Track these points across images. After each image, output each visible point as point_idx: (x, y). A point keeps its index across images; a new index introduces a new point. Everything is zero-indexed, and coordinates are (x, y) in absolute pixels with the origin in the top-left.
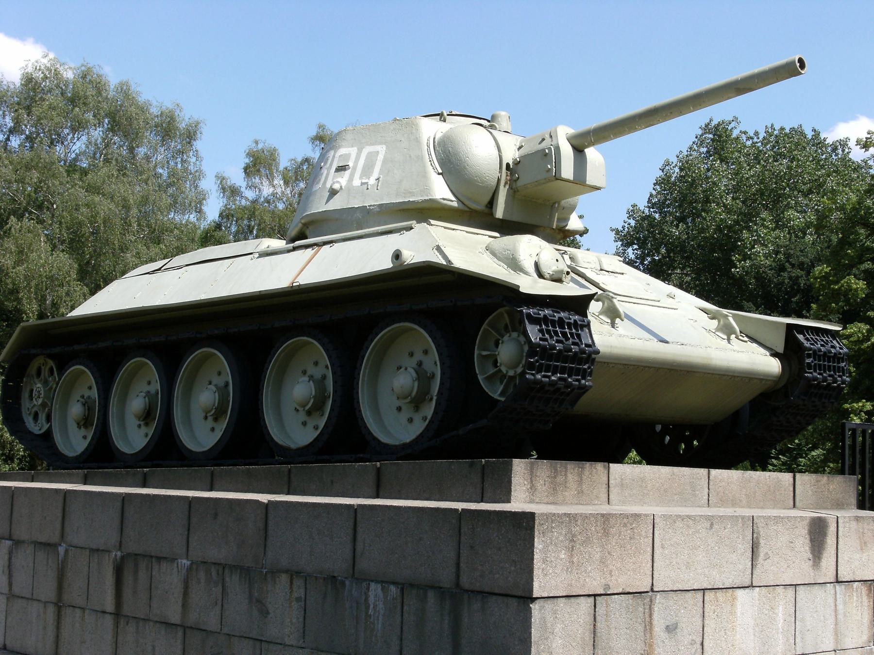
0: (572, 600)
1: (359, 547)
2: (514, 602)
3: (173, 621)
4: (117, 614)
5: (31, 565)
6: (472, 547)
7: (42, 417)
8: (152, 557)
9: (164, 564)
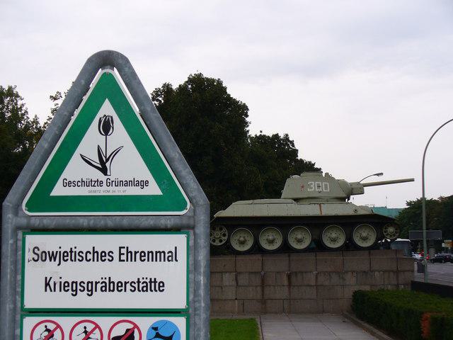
7: (217, 241)
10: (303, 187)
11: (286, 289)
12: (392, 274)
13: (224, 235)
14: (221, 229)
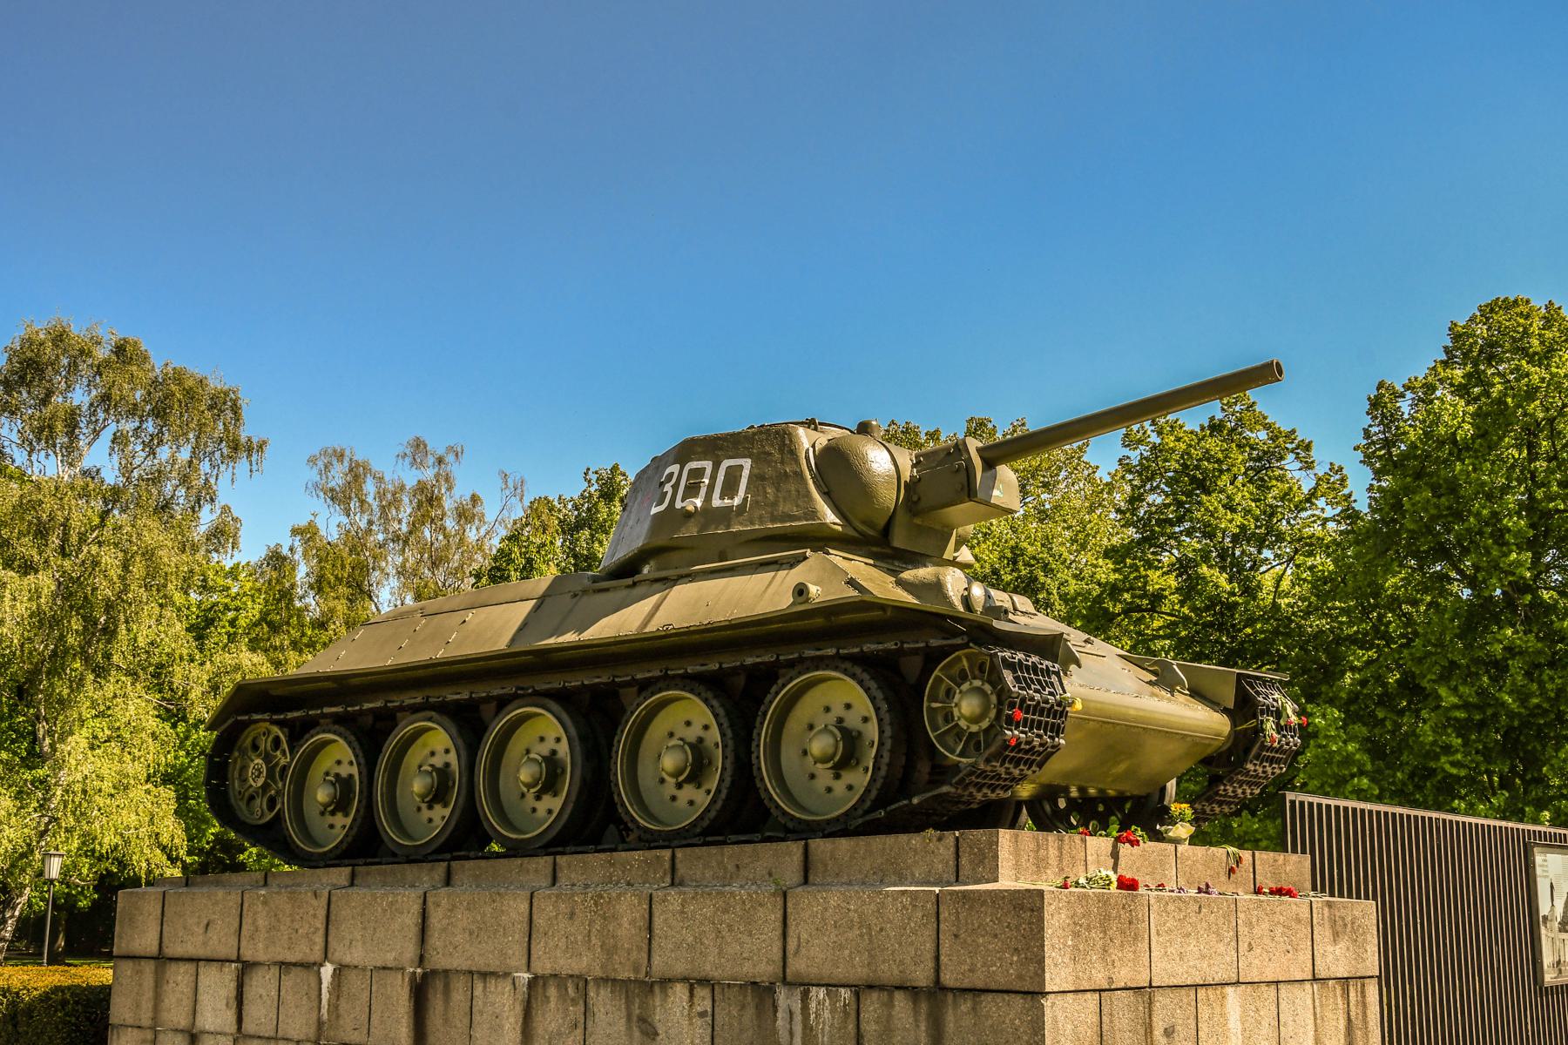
0: (1080, 995)
2: (1018, 1001)
5: (274, 993)
6: (956, 936)
8: (471, 972)
12: (901, 1001)
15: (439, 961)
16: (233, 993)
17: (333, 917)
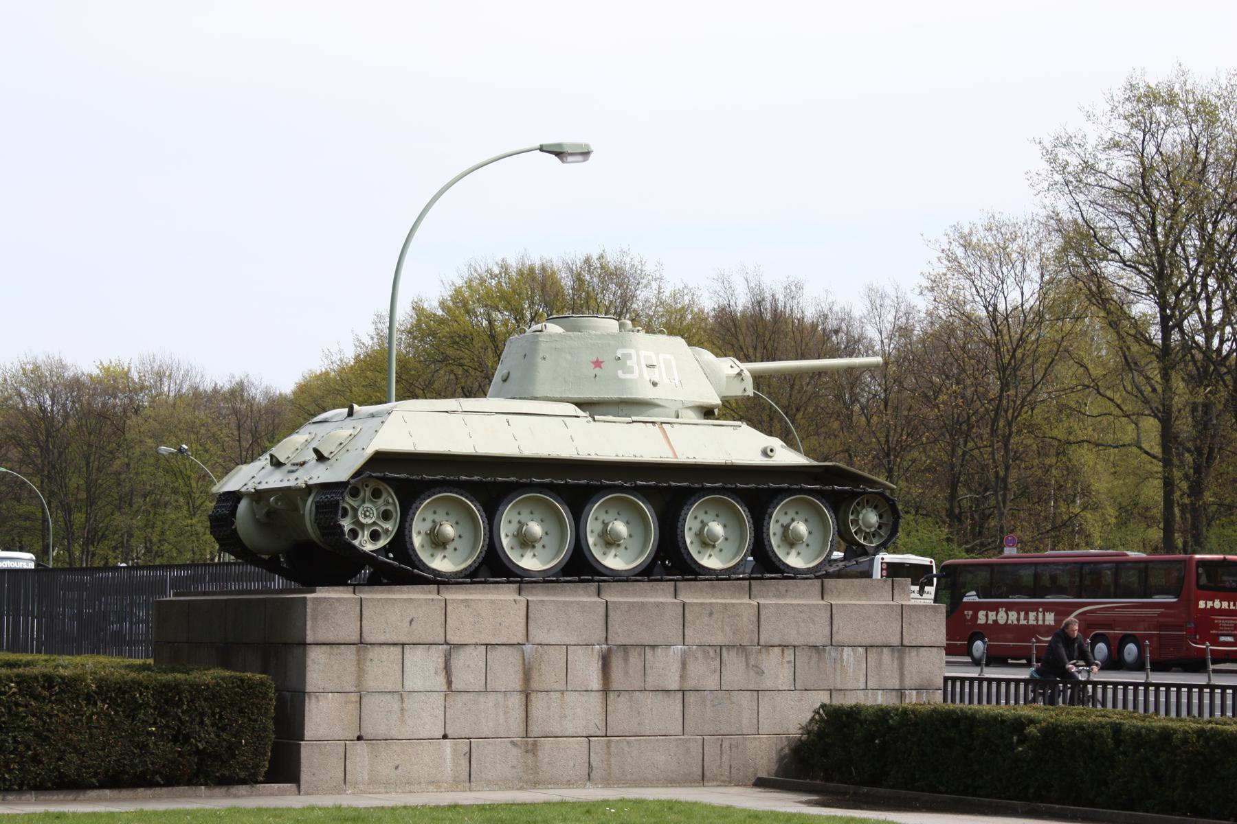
1: (835, 629)
3: (672, 688)
4: (606, 690)
9: (659, 650)
10: (598, 364)
11: (596, 700)
13: (386, 516)
14: (376, 494)
15: (618, 637)
16: (442, 665)
17: (531, 615)
